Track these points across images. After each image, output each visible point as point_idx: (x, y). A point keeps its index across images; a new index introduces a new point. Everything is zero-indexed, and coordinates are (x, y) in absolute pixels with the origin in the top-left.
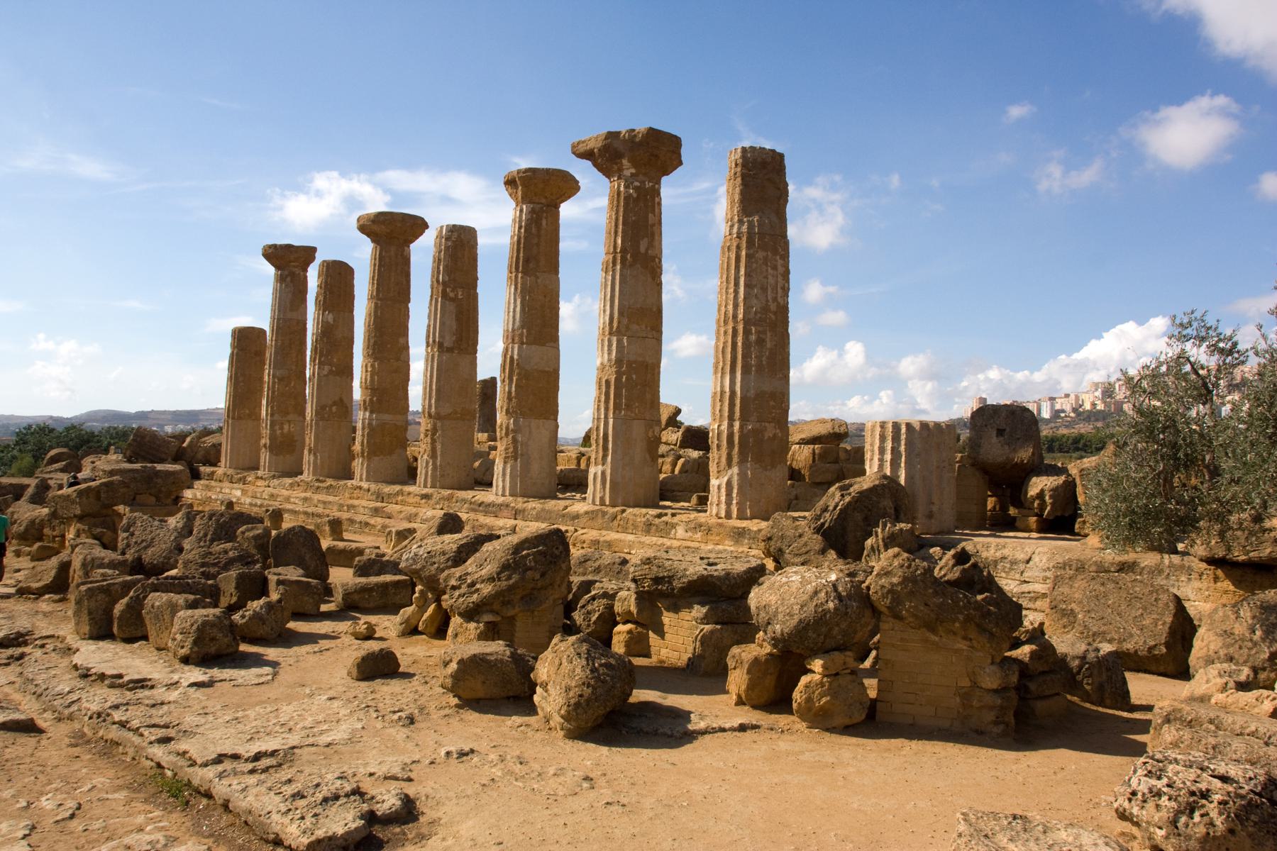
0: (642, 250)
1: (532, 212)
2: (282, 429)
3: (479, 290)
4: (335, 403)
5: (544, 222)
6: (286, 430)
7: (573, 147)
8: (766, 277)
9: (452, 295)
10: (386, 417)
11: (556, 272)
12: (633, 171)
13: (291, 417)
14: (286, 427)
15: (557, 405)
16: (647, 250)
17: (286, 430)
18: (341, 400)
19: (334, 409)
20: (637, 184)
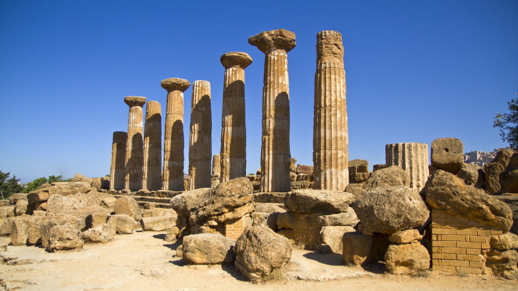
0: (280, 82)
1: (233, 70)
2: (133, 171)
3: (211, 108)
4: (154, 159)
5: (238, 75)
6: (135, 172)
7: (249, 40)
8: (336, 87)
9: (200, 109)
10: (175, 163)
11: (244, 97)
12: (275, 48)
13: (136, 167)
14: (135, 170)
15: (245, 152)
16: (282, 81)
17: (135, 172)
18: (157, 158)
19: (154, 161)
20: (277, 54)
